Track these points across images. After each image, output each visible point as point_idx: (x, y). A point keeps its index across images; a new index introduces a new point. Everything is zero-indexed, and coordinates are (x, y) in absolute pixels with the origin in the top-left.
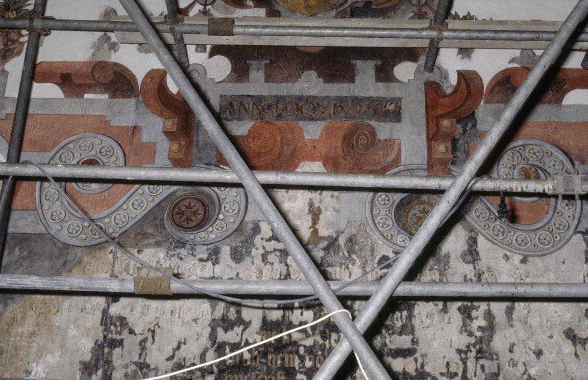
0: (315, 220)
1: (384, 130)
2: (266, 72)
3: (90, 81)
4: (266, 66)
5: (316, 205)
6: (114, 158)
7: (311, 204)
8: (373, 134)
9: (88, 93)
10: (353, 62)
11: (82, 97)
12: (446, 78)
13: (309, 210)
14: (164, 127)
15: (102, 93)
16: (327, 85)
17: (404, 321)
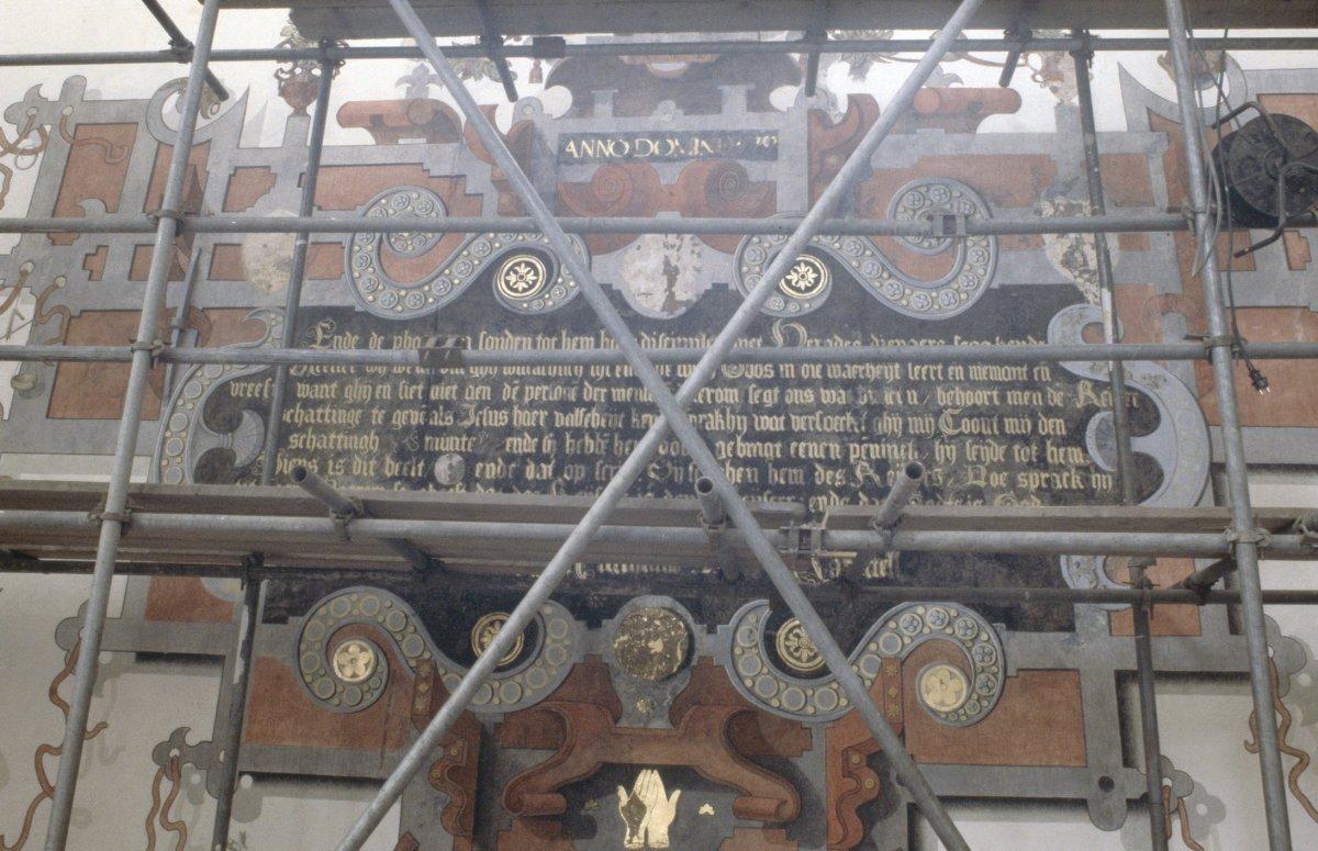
0: (671, 282)
1: (756, 170)
2: (614, 104)
3: (405, 123)
4: (615, 97)
5: (673, 263)
6: (434, 214)
7: (667, 263)
8: (743, 174)
9: (402, 138)
10: (721, 87)
11: (397, 143)
12: (834, 104)
13: (665, 270)
14: (492, 175)
15: (419, 137)
16: (687, 118)
17: (776, 400)
